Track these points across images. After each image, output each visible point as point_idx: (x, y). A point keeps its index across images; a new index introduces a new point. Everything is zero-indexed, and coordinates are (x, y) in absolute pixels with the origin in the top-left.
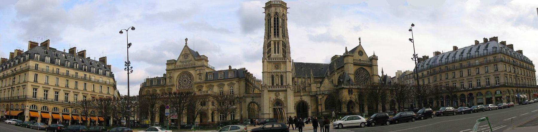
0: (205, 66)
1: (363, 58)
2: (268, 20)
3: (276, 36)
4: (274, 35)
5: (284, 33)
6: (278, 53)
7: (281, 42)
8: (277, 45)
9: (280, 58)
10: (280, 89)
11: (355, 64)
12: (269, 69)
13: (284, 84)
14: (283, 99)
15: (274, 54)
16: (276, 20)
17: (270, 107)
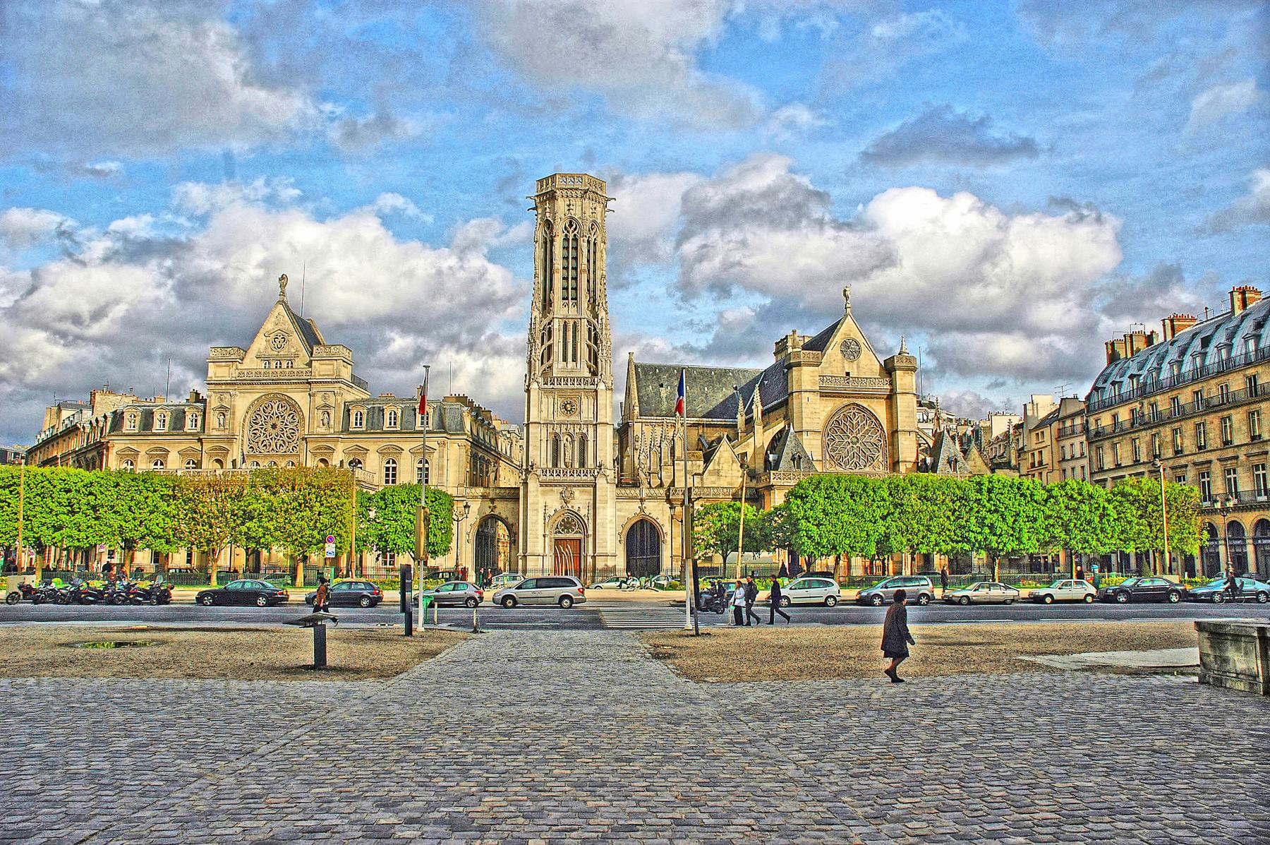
0: (342, 382)
1: (858, 367)
2: (546, 243)
3: (571, 304)
4: (563, 299)
5: (594, 292)
6: (574, 359)
7: (585, 322)
8: (570, 334)
9: (579, 379)
10: (576, 478)
11: (824, 394)
12: (544, 415)
13: (590, 463)
14: (583, 512)
15: (562, 364)
16: (572, 245)
17: (544, 536)
